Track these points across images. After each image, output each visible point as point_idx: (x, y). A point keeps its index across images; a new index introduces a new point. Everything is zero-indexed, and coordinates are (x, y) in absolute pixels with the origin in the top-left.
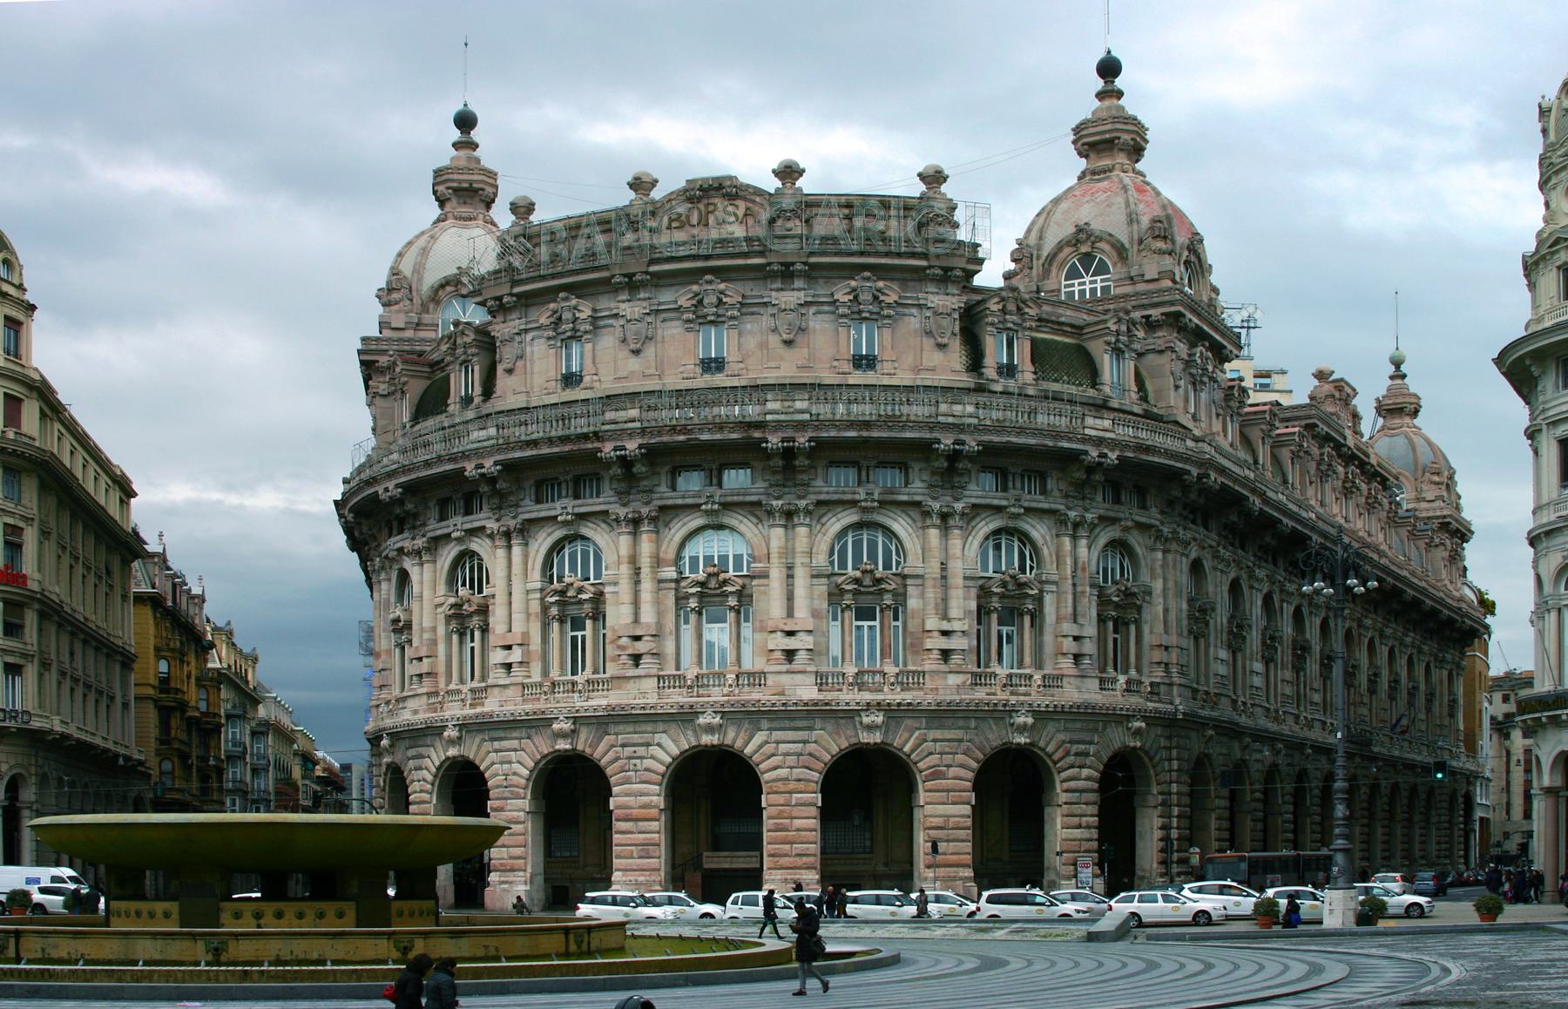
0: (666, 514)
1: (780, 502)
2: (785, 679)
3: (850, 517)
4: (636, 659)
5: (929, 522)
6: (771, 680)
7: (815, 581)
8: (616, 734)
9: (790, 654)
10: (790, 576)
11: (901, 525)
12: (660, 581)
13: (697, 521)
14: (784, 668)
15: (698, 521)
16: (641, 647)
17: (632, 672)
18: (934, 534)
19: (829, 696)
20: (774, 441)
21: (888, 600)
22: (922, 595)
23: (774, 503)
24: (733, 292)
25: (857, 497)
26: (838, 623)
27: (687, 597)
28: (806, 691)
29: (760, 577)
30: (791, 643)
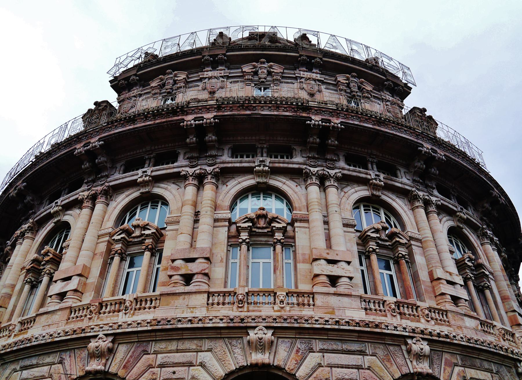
0: (224, 175)
1: (316, 169)
2: (334, 301)
3: (363, 192)
4: (188, 279)
5: (417, 204)
6: (319, 300)
7: (346, 229)
8: (156, 353)
9: (334, 280)
10: (326, 223)
11: (399, 204)
12: (216, 220)
13: (248, 181)
14: (332, 290)
15: (248, 181)
16: (194, 268)
17: (182, 289)
18: (422, 211)
19: (378, 319)
20: (316, 119)
21: (402, 251)
22: (424, 254)
23: (312, 169)
24: (277, 69)
25: (369, 177)
26: (364, 268)
27: (239, 230)
28: (354, 312)
29: (301, 221)
30: (334, 270)
